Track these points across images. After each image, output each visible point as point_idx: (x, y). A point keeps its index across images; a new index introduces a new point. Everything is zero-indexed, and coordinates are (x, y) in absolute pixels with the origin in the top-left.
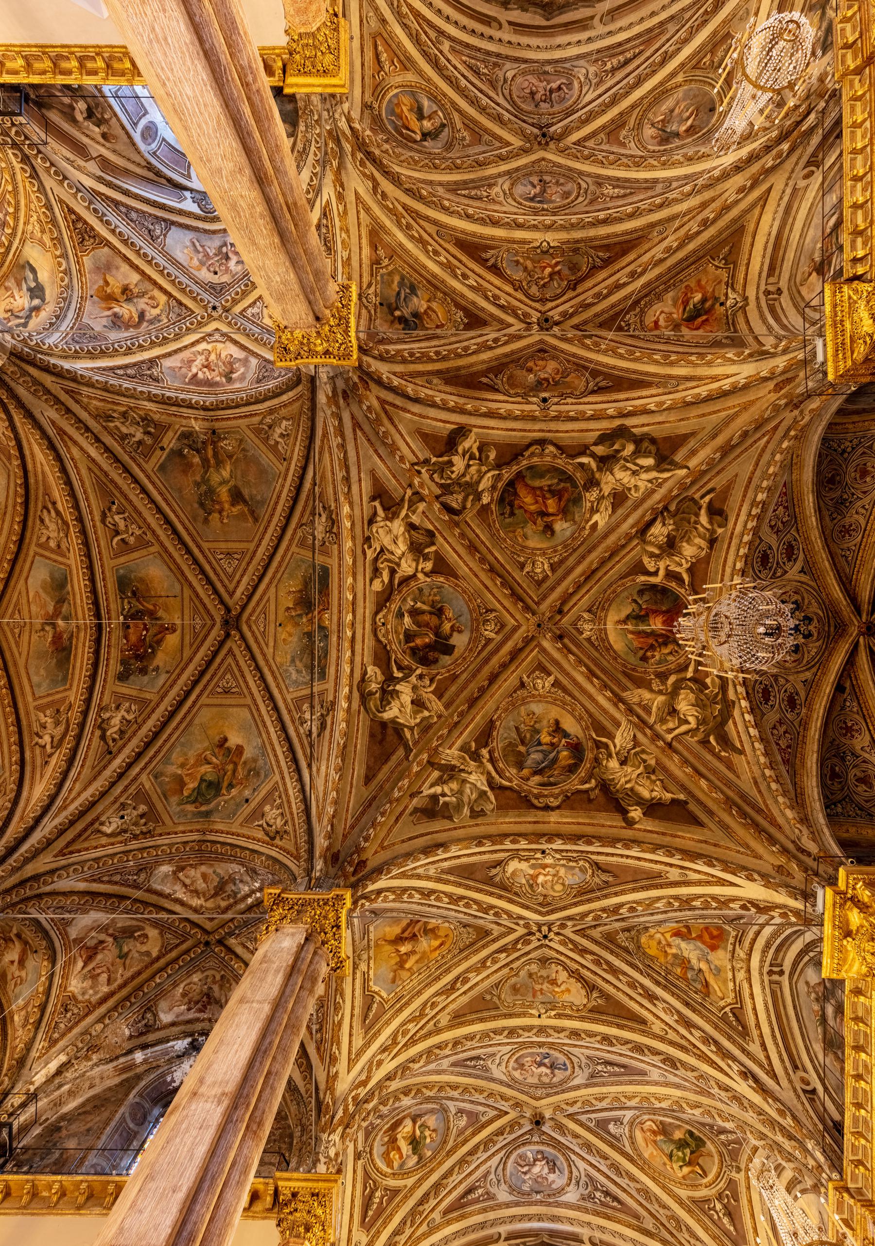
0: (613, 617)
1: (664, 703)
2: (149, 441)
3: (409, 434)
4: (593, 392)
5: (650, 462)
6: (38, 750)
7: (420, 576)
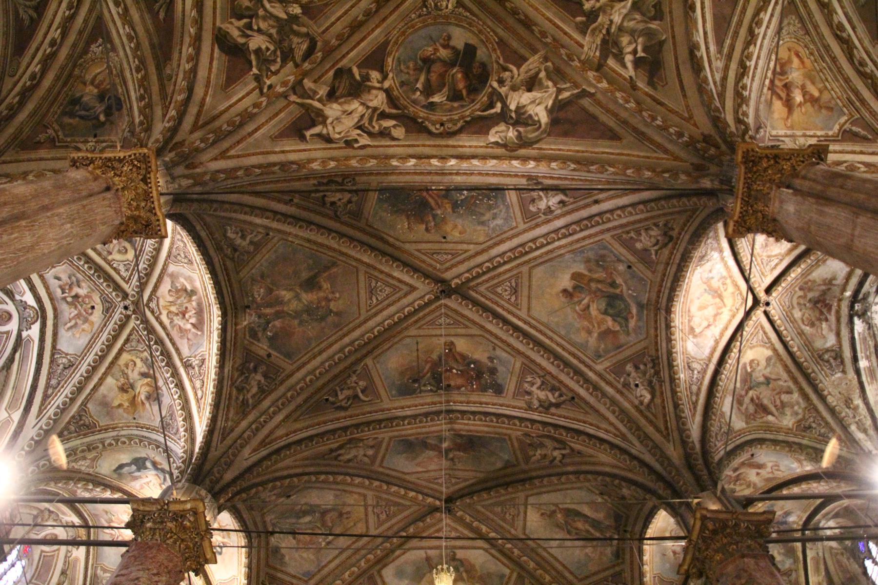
2: (262, 369)
3: (229, 97)
6: (568, 460)
7: (386, 84)
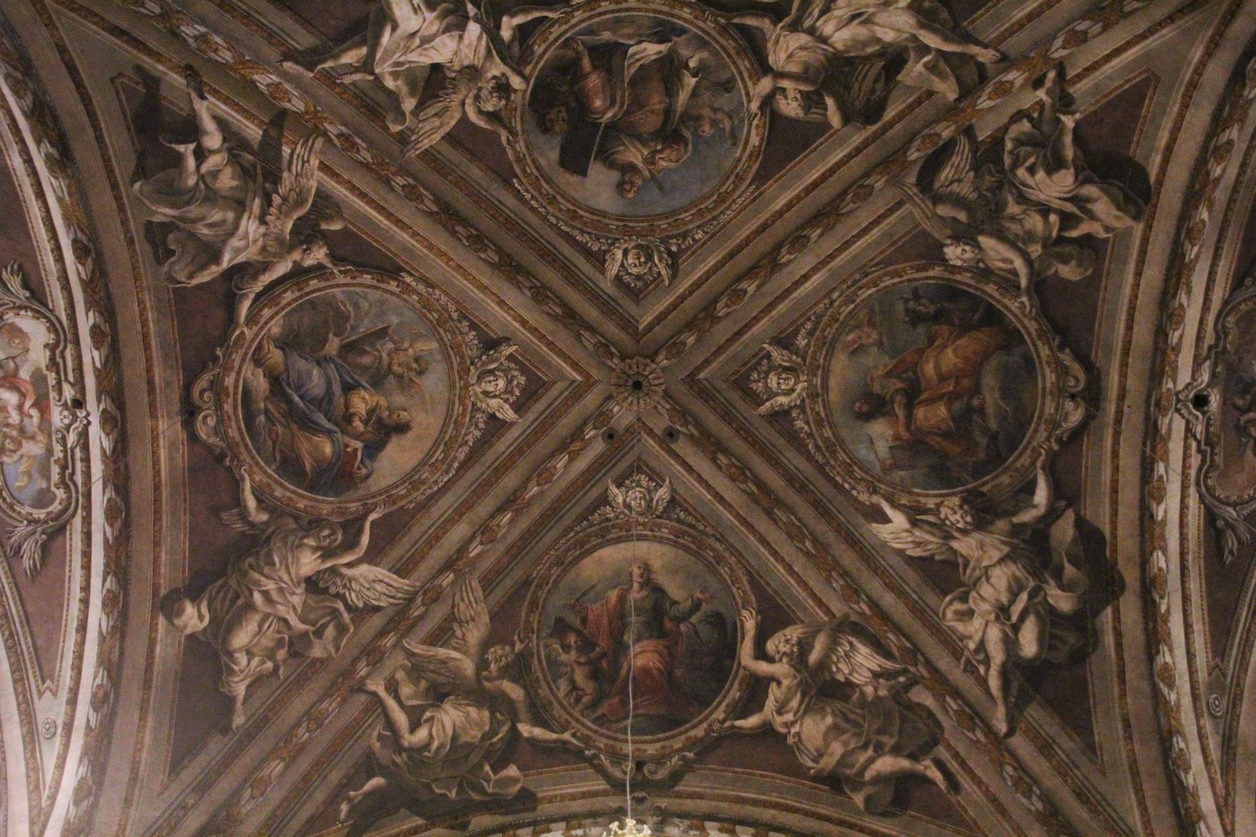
0: (658, 555)
1: (457, 674)
3: (1147, 56)
4: (1210, 517)
5: (1029, 644)
7: (766, 84)
